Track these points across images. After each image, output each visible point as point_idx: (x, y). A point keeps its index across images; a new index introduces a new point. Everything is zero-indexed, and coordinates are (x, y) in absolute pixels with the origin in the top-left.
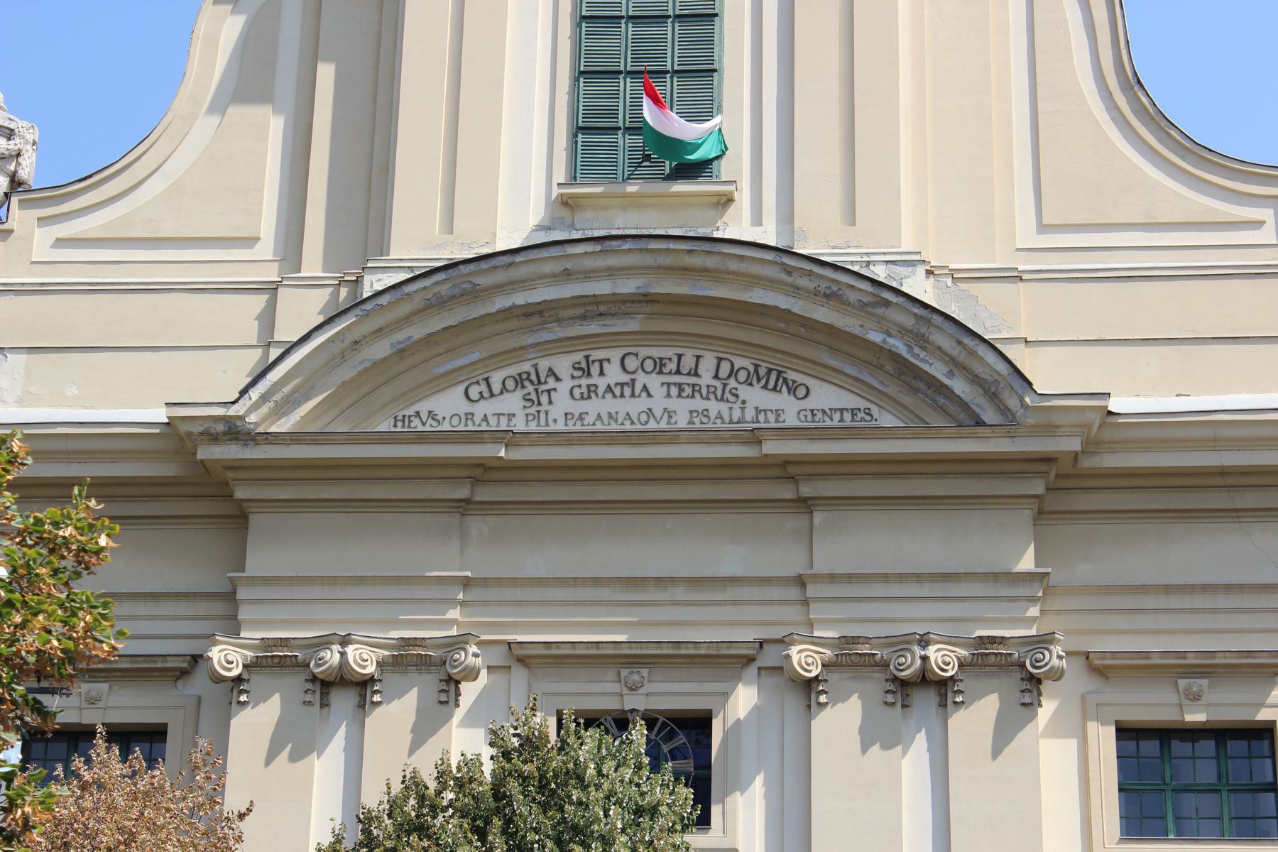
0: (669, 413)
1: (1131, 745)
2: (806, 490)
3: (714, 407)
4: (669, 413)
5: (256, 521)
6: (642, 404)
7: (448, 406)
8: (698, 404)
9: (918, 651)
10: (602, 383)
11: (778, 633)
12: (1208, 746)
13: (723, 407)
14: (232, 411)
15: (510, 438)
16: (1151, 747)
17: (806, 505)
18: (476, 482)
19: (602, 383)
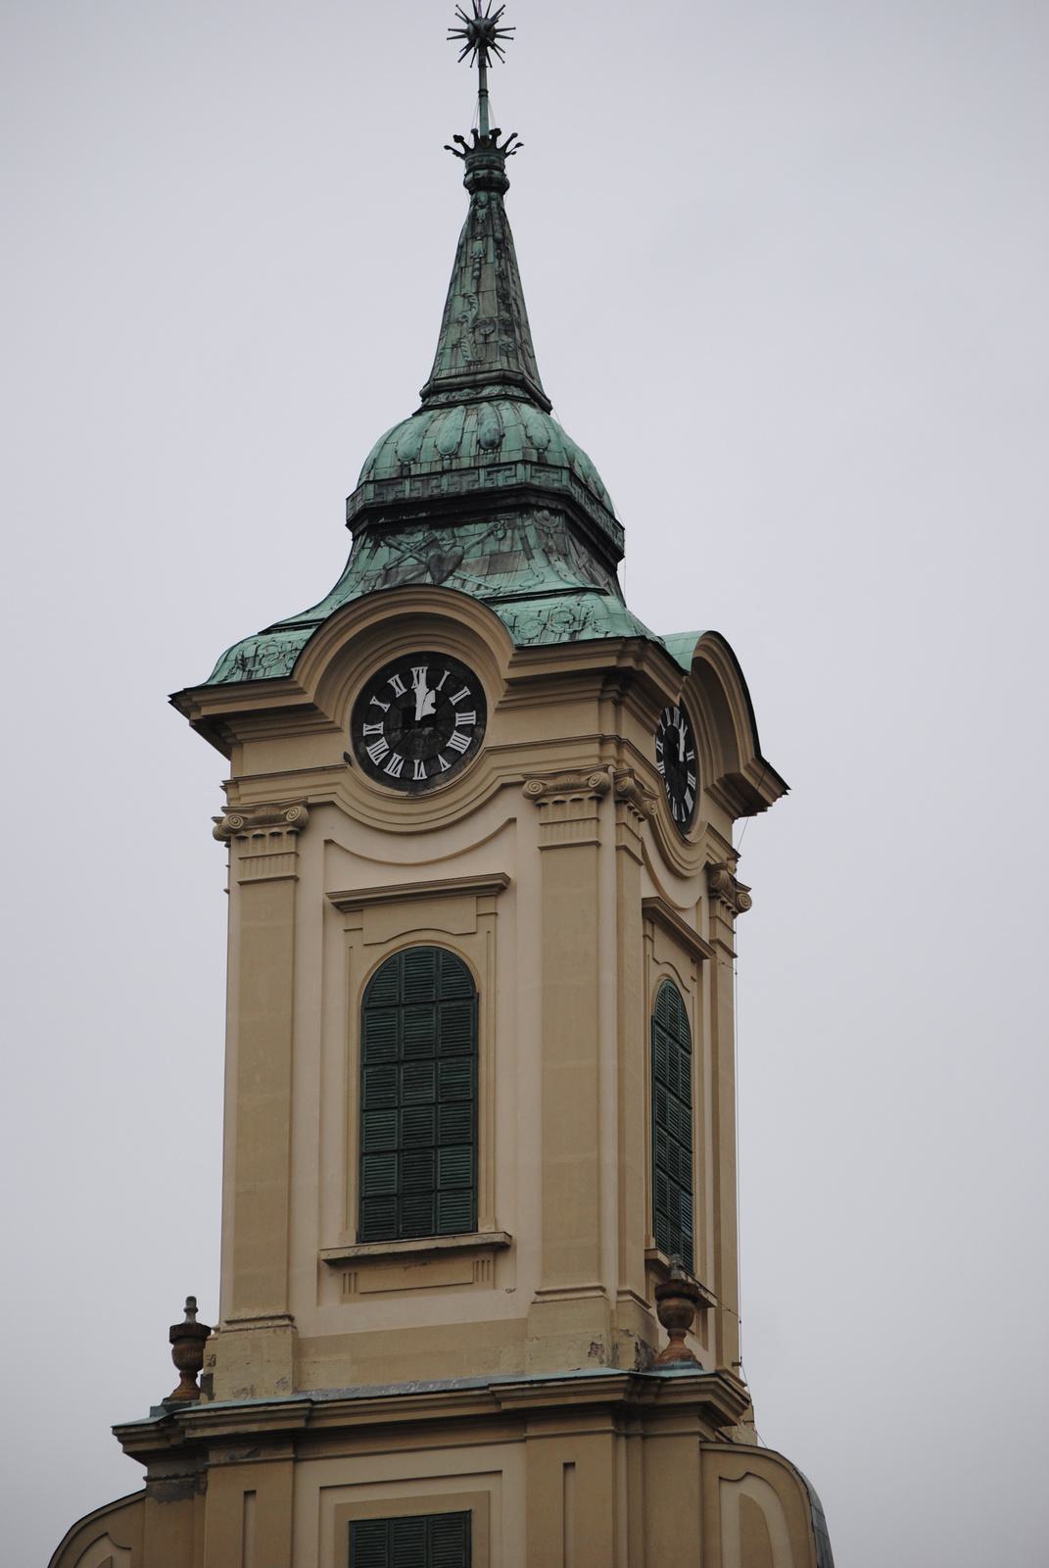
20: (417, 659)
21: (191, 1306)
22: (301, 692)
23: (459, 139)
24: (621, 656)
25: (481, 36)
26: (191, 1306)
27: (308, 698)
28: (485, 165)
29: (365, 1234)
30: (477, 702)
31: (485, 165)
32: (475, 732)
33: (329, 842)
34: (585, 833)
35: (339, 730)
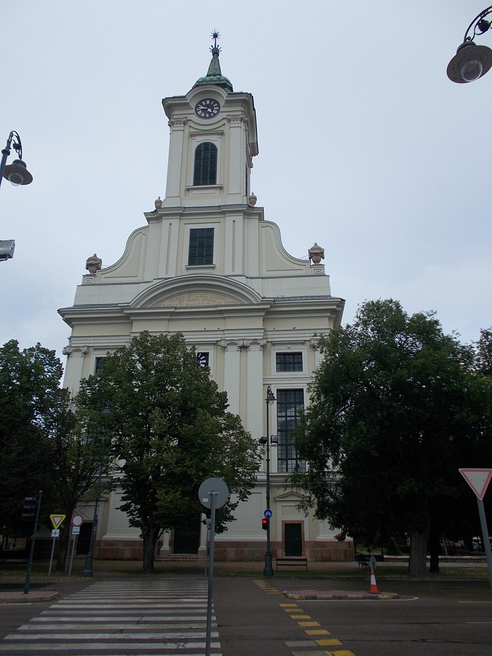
0: (203, 303)
1: (278, 357)
2: (225, 315)
3: (210, 302)
4: (203, 303)
5: (134, 323)
6: (199, 302)
7: (167, 303)
8: (208, 302)
9: (242, 342)
10: (192, 299)
11: (219, 339)
12: (292, 356)
13: (212, 302)
14: (130, 304)
15: (176, 308)
16: (282, 357)
17: (225, 318)
18: (171, 316)
19: (192, 299)
20: (208, 99)
21: (159, 198)
22: (187, 100)
23: (212, 46)
24: (247, 97)
25: (215, 36)
26: (159, 198)
27: (188, 101)
28: (216, 52)
29: (195, 184)
30: (219, 106)
31: (216, 52)
32: (218, 111)
33: (190, 126)
34: (239, 125)
35: (193, 109)
